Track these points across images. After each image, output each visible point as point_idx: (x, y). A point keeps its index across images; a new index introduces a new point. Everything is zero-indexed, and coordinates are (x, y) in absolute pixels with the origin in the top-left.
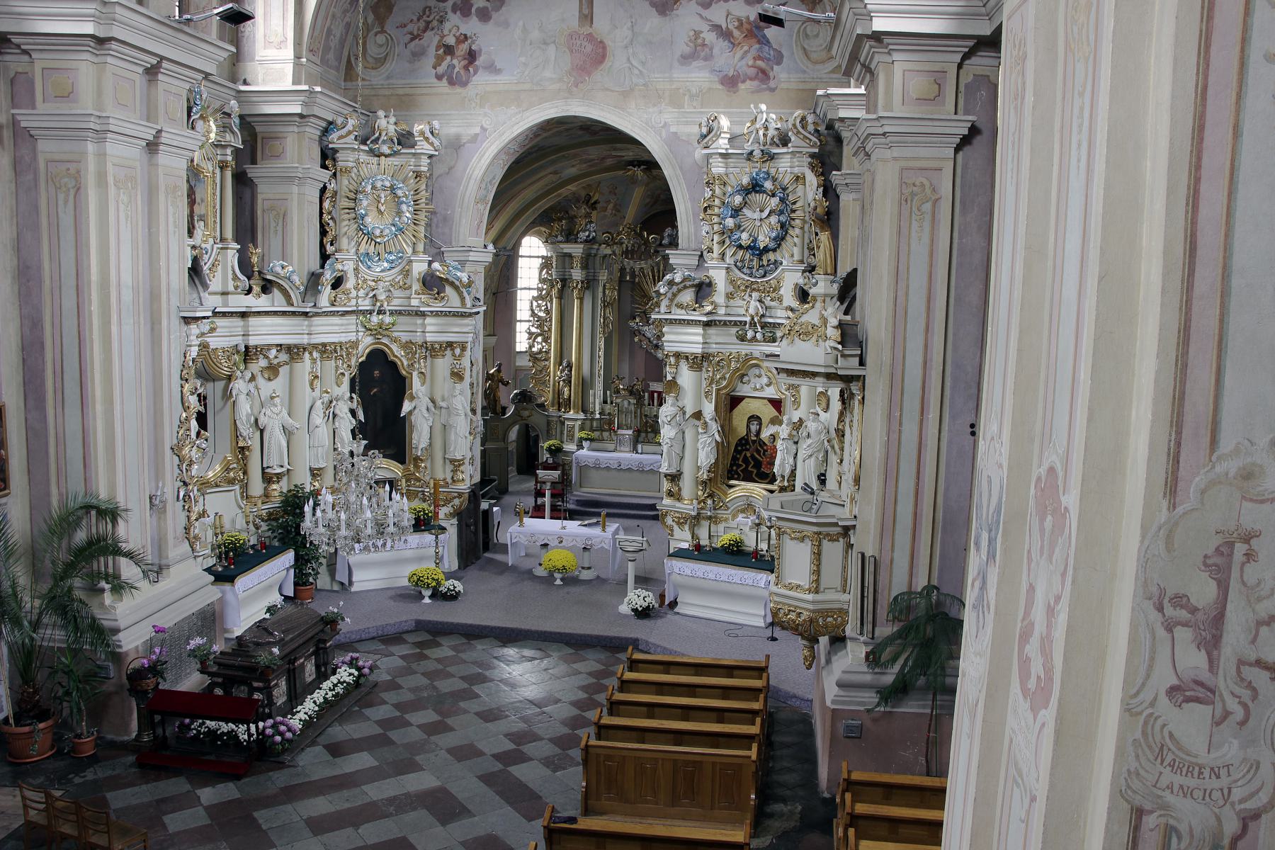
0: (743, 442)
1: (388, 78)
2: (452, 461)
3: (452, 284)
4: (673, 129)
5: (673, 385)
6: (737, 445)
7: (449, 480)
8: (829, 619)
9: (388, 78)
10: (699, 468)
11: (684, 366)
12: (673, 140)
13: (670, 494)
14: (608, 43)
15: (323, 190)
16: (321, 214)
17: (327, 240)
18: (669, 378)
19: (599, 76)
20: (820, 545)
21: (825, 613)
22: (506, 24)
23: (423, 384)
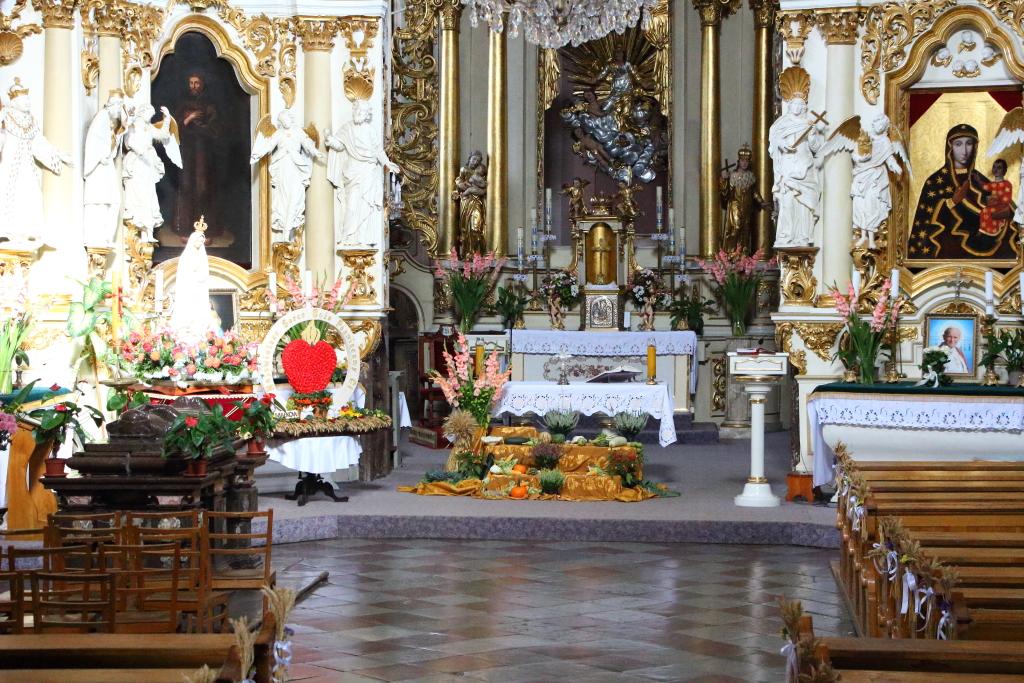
0: (937, 184)
2: (347, 256)
5: (799, 74)
10: (857, 232)
11: (815, 34)
13: (798, 292)
23: (289, 104)
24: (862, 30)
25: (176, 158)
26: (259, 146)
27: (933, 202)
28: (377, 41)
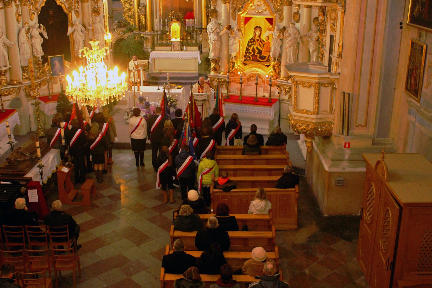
0: (252, 41)
6: (249, 42)
8: (324, 127)
18: (212, 8)
20: (319, 90)
21: (321, 124)
26: (70, 30)
27: (250, 46)
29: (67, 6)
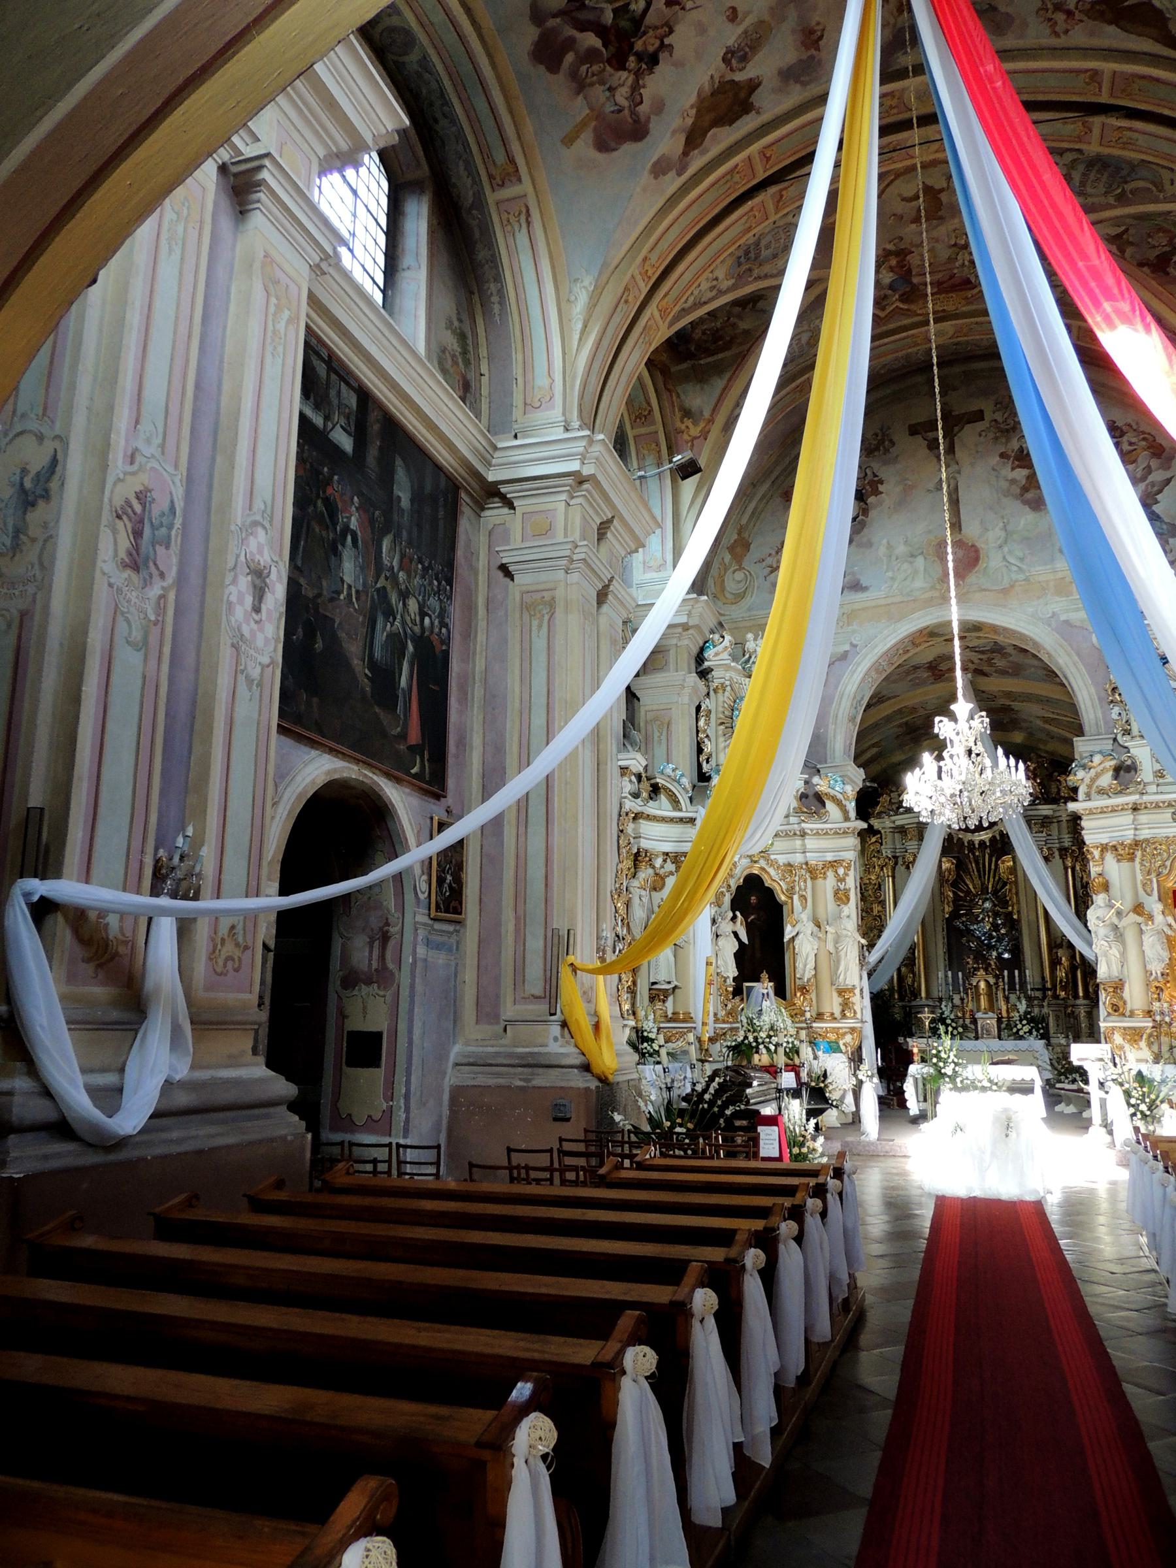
1: (749, 610)
3: (834, 799)
4: (1063, 617)
7: (837, 1014)
9: (749, 610)
10: (1148, 973)
11: (1110, 857)
12: (1066, 629)
14: (980, 545)
15: (698, 708)
16: (698, 732)
17: (703, 758)
19: (972, 578)
22: (870, 545)
23: (804, 908)
24: (1139, 854)
25: (745, 940)
28: (851, 873)
29: (784, 887)
